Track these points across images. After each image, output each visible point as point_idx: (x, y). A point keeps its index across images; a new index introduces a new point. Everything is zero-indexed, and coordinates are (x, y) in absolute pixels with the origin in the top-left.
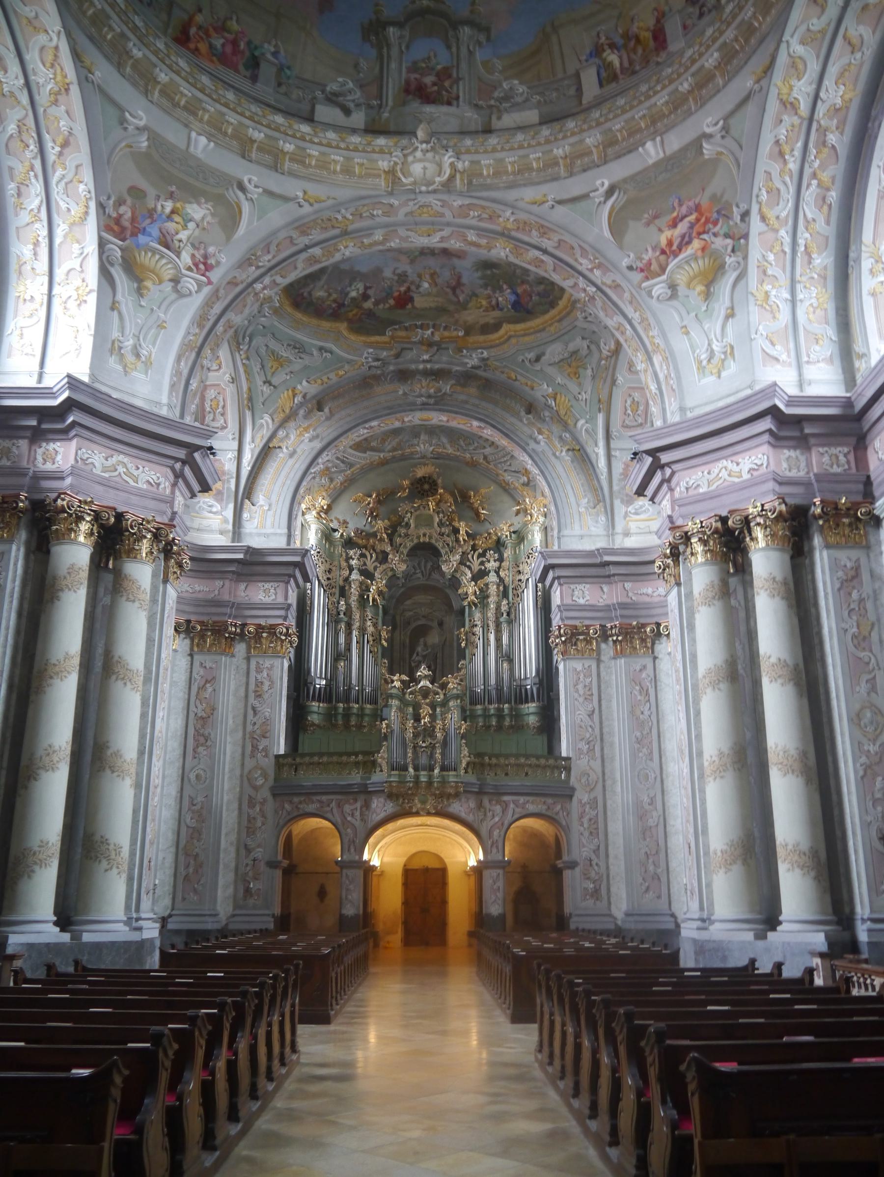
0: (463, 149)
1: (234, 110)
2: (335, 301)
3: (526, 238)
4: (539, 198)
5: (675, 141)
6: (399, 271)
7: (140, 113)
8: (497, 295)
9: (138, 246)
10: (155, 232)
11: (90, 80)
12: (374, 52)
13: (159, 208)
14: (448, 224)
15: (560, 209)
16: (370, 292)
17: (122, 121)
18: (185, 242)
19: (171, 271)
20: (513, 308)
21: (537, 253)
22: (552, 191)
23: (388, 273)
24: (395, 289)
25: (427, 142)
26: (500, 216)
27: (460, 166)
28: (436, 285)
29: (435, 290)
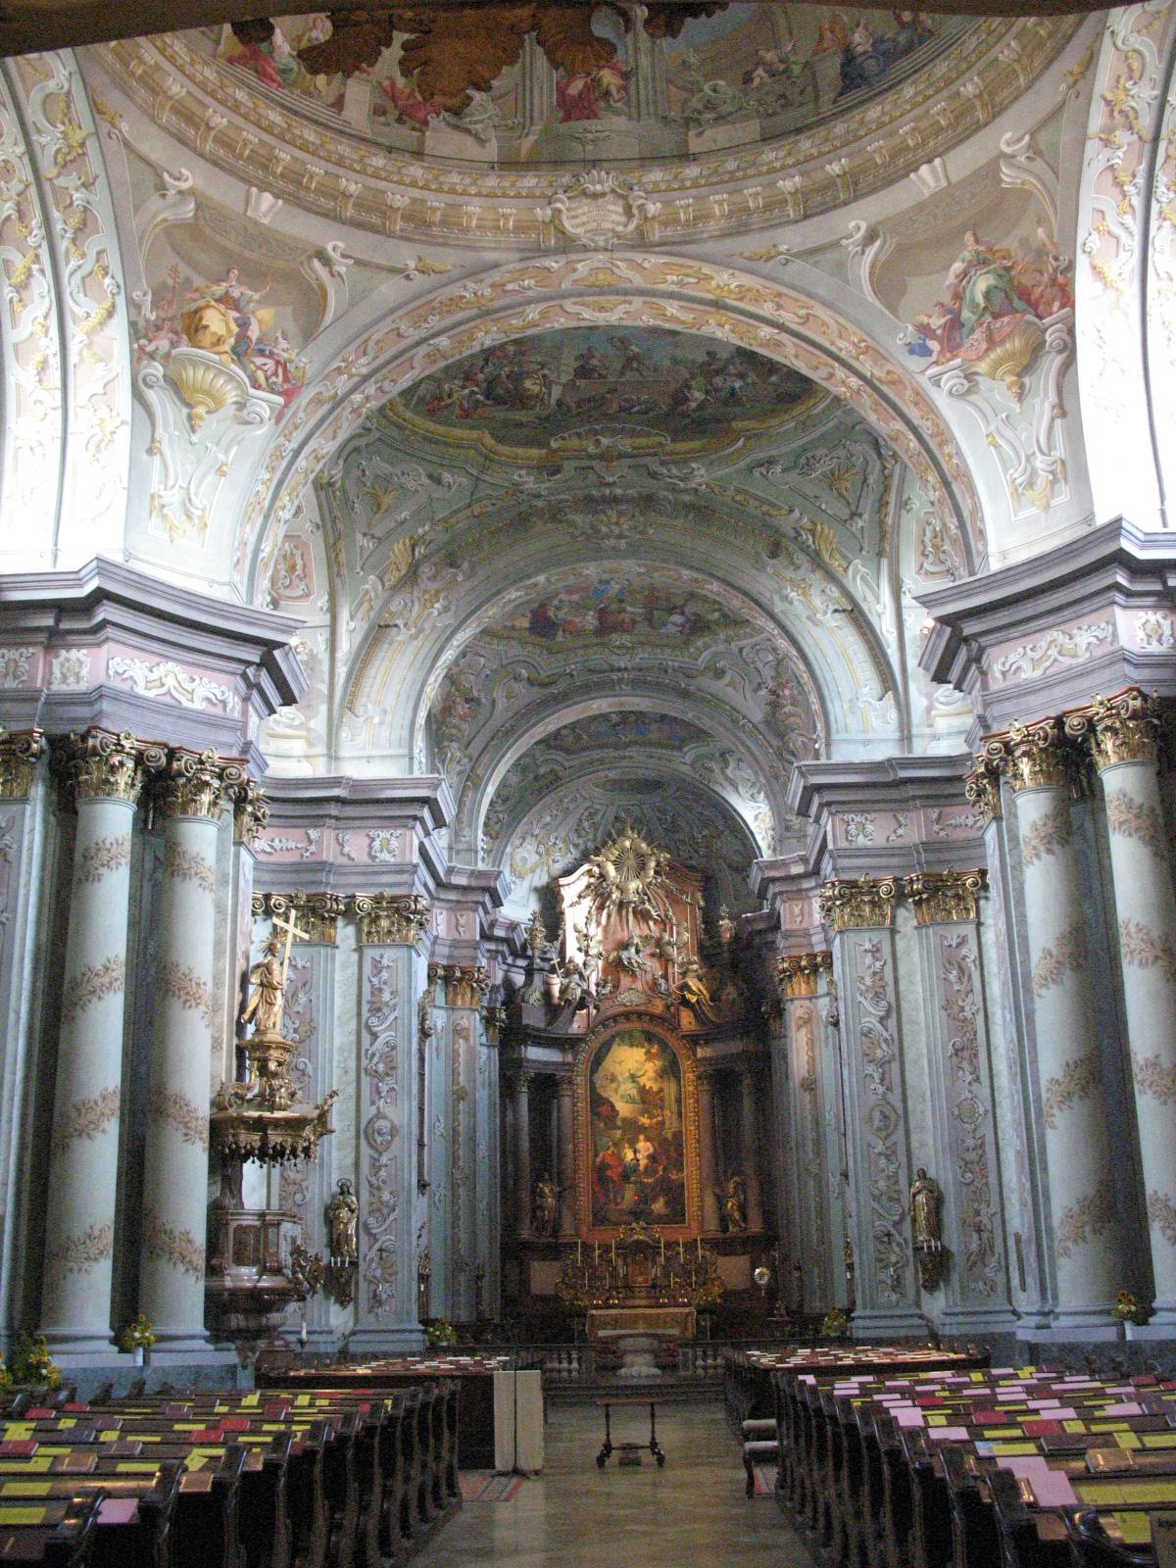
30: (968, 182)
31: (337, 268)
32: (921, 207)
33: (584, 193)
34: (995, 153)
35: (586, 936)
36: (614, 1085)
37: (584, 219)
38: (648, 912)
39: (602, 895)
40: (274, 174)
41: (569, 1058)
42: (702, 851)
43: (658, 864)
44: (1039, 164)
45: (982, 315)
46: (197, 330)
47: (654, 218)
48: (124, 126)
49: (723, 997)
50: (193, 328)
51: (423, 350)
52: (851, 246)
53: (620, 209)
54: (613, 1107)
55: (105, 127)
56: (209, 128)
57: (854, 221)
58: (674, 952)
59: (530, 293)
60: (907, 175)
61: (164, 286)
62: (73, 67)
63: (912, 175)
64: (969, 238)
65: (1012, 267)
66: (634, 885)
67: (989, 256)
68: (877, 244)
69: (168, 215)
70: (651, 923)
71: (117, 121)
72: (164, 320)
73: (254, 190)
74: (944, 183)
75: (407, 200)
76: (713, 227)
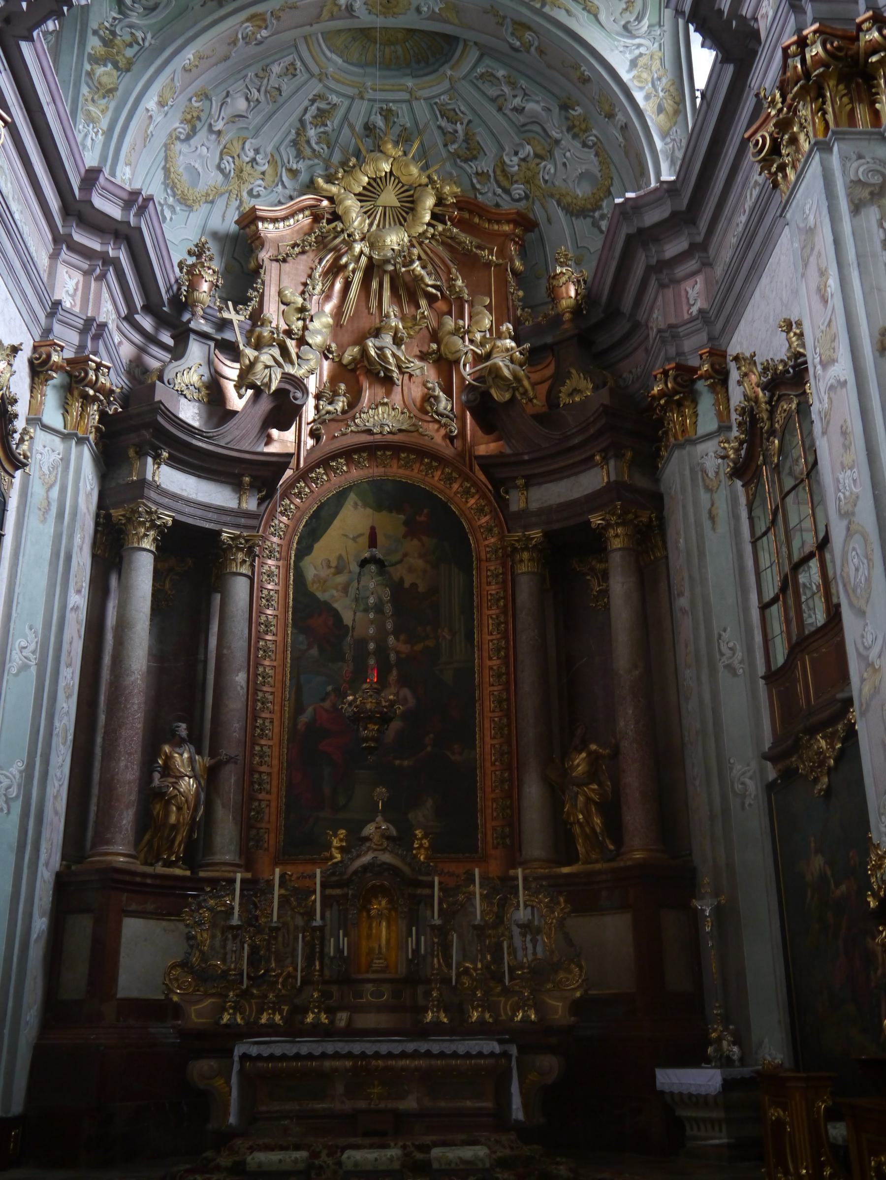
35: (302, 310)
36: (341, 579)
38: (419, 279)
39: (335, 249)
41: (251, 504)
42: (518, 190)
43: (440, 202)
49: (564, 399)
54: (337, 616)
58: (464, 347)
66: (395, 239)
70: (423, 303)
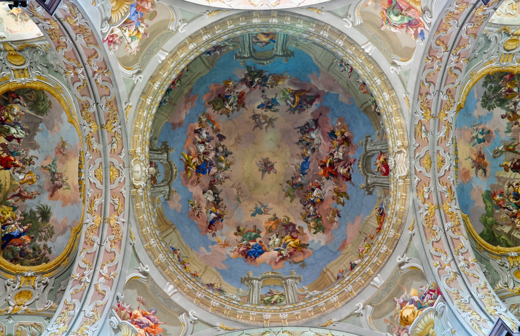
0: (145, 191)
1: (167, 77)
2: (8, 118)
3: (105, 233)
4: (133, 235)
5: (178, 299)
6: (34, 159)
7: (184, 31)
8: (16, 223)
9: (132, 6)
10: (134, 18)
11: (206, 12)
12: (159, 147)
13: (142, 25)
14: (106, 187)
15: (131, 247)
16: (14, 142)
17: (184, 20)
18: (124, 33)
19: (114, 20)
20: (5, 235)
21: (98, 240)
22: (137, 241)
23: (32, 153)
24: (17, 157)
25: (148, 173)
26: (118, 215)
27: (140, 190)
28: (21, 184)
29: (17, 183)
30: (365, 34)
31: (406, 260)
32: (380, 49)
33: (394, 167)
34: (353, 28)
37: (402, 168)
40: (373, 274)
44: (350, 12)
45: (404, 15)
46: (407, 320)
47: (402, 143)
48: (334, 320)
50: (406, 321)
51: (450, 233)
52: (399, 71)
53: (399, 155)
55: (331, 326)
56: (351, 292)
57: (391, 71)
59: (432, 189)
60: (370, 57)
61: (388, 327)
62: (308, 329)
63: (370, 55)
64: (383, 29)
65: (384, 9)
67: (385, 20)
68: (396, 61)
69: (368, 315)
71: (332, 321)
72: (398, 332)
73: (372, 283)
74: (370, 43)
75: (392, 230)
76: (403, 122)
